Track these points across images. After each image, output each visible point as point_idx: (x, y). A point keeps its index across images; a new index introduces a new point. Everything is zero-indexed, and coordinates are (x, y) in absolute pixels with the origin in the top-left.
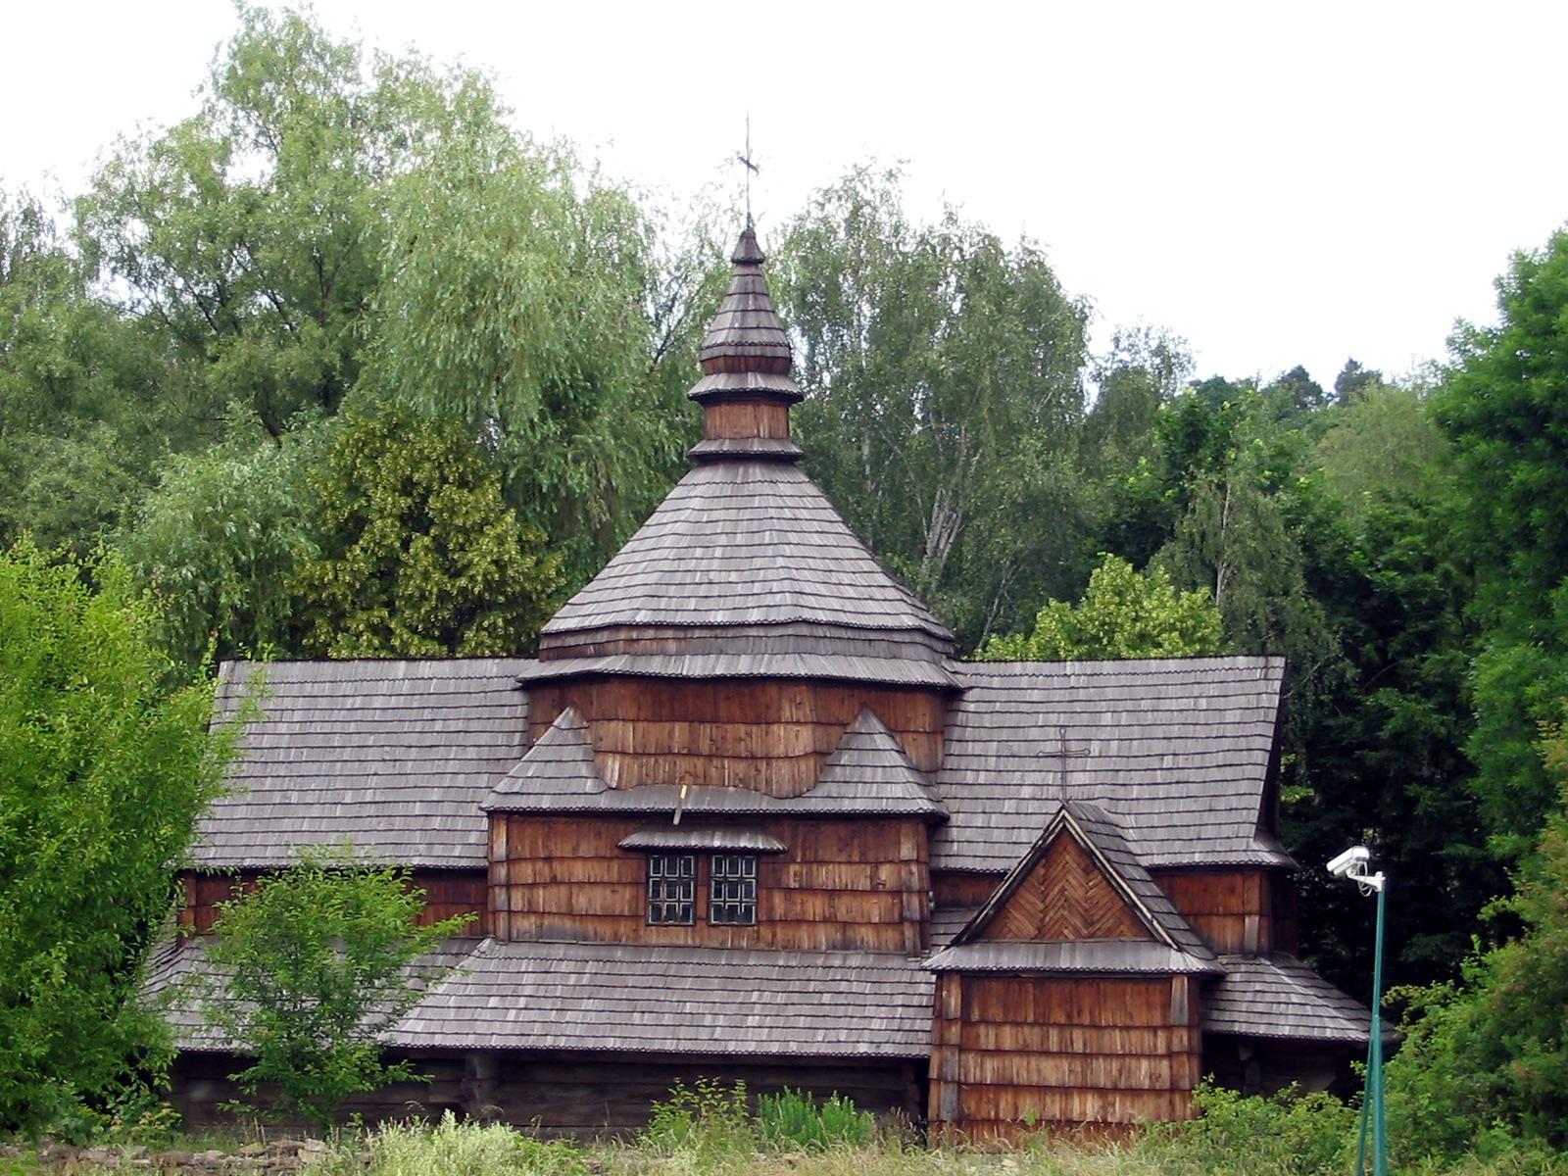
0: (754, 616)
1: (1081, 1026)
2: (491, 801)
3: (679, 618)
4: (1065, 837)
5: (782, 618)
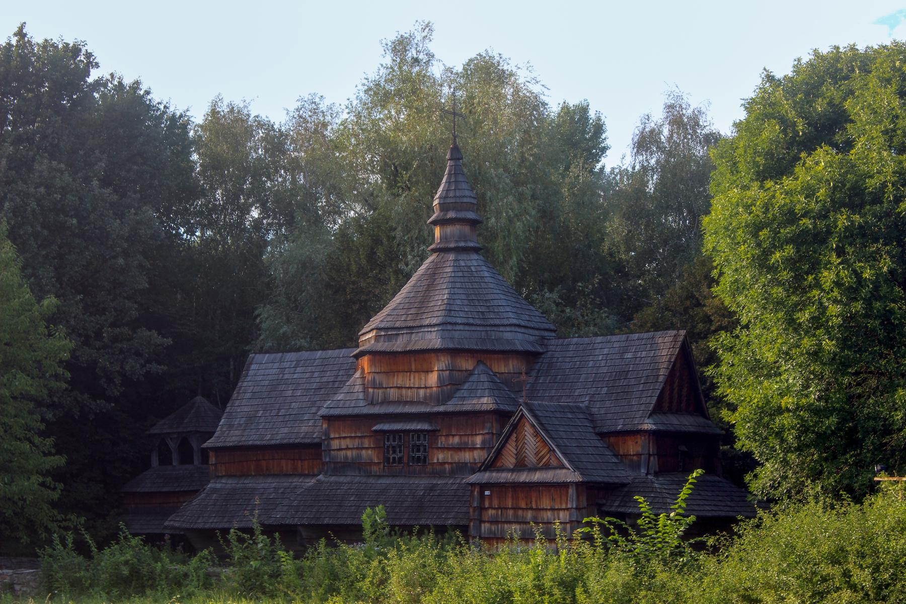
0: (427, 322)
1: (531, 509)
2: (323, 412)
3: (398, 325)
4: (524, 420)
5: (438, 322)
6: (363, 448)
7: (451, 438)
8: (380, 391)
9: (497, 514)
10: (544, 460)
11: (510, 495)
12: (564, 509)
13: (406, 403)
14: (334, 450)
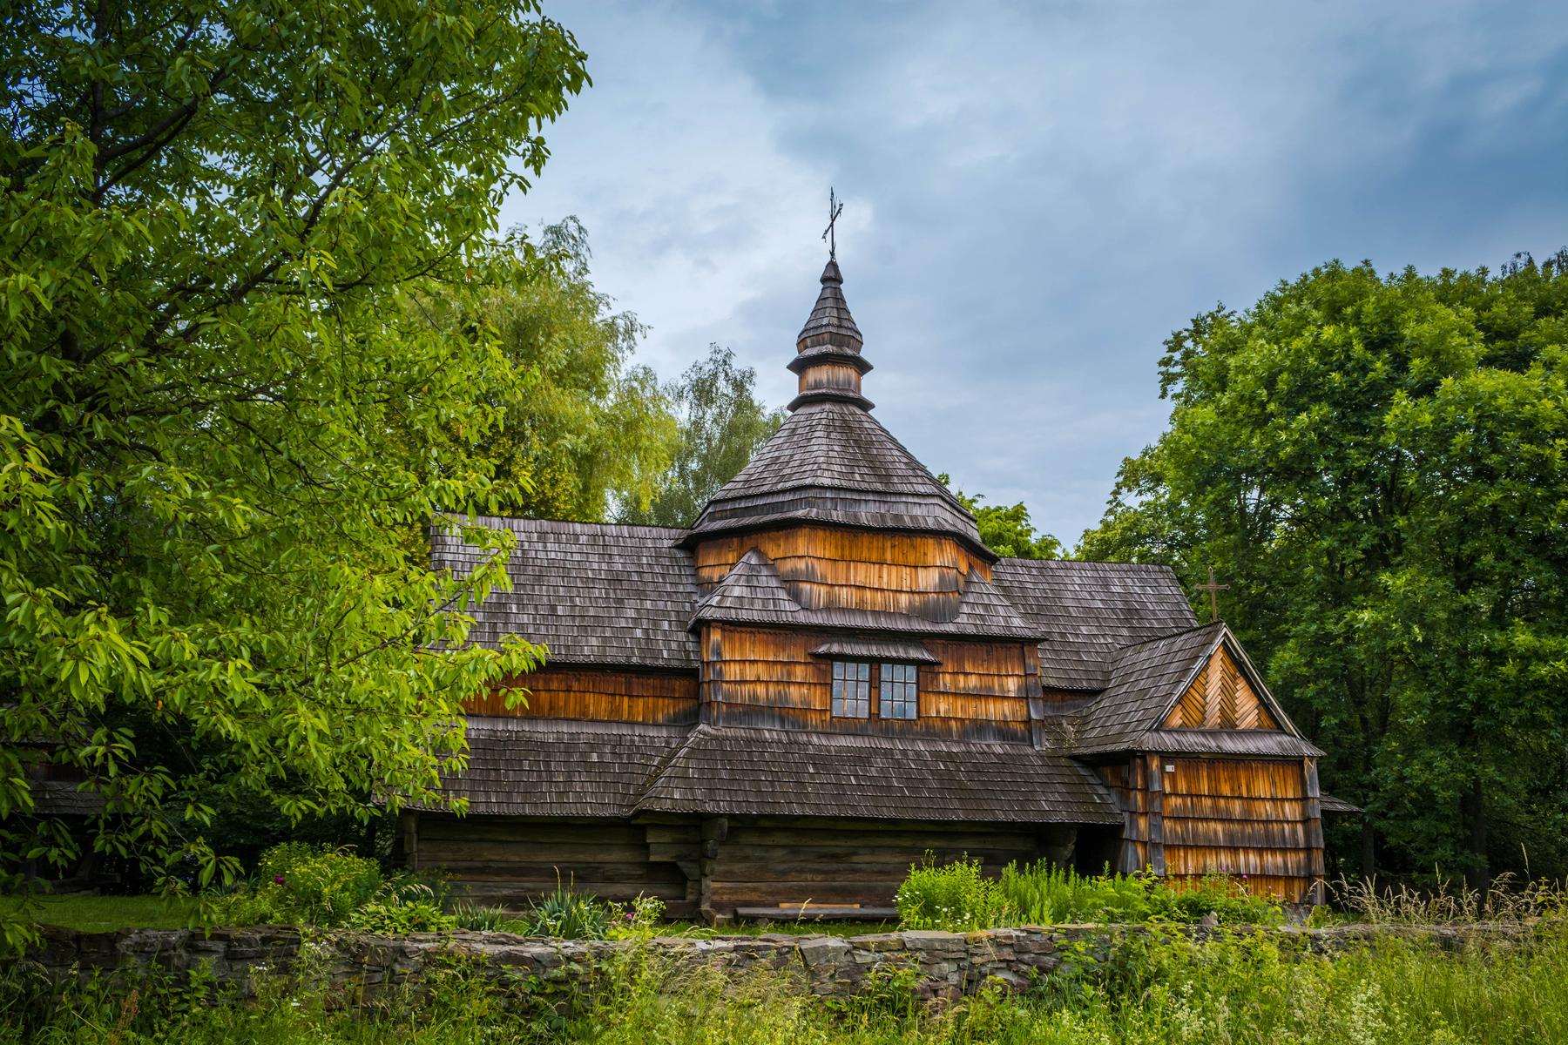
0: (906, 488)
1: (1240, 797)
6: (789, 683)
7: (961, 678)
8: (823, 589)
9: (1185, 804)
10: (1249, 719)
11: (1205, 774)
12: (1291, 800)
13: (875, 613)
14: (727, 682)
